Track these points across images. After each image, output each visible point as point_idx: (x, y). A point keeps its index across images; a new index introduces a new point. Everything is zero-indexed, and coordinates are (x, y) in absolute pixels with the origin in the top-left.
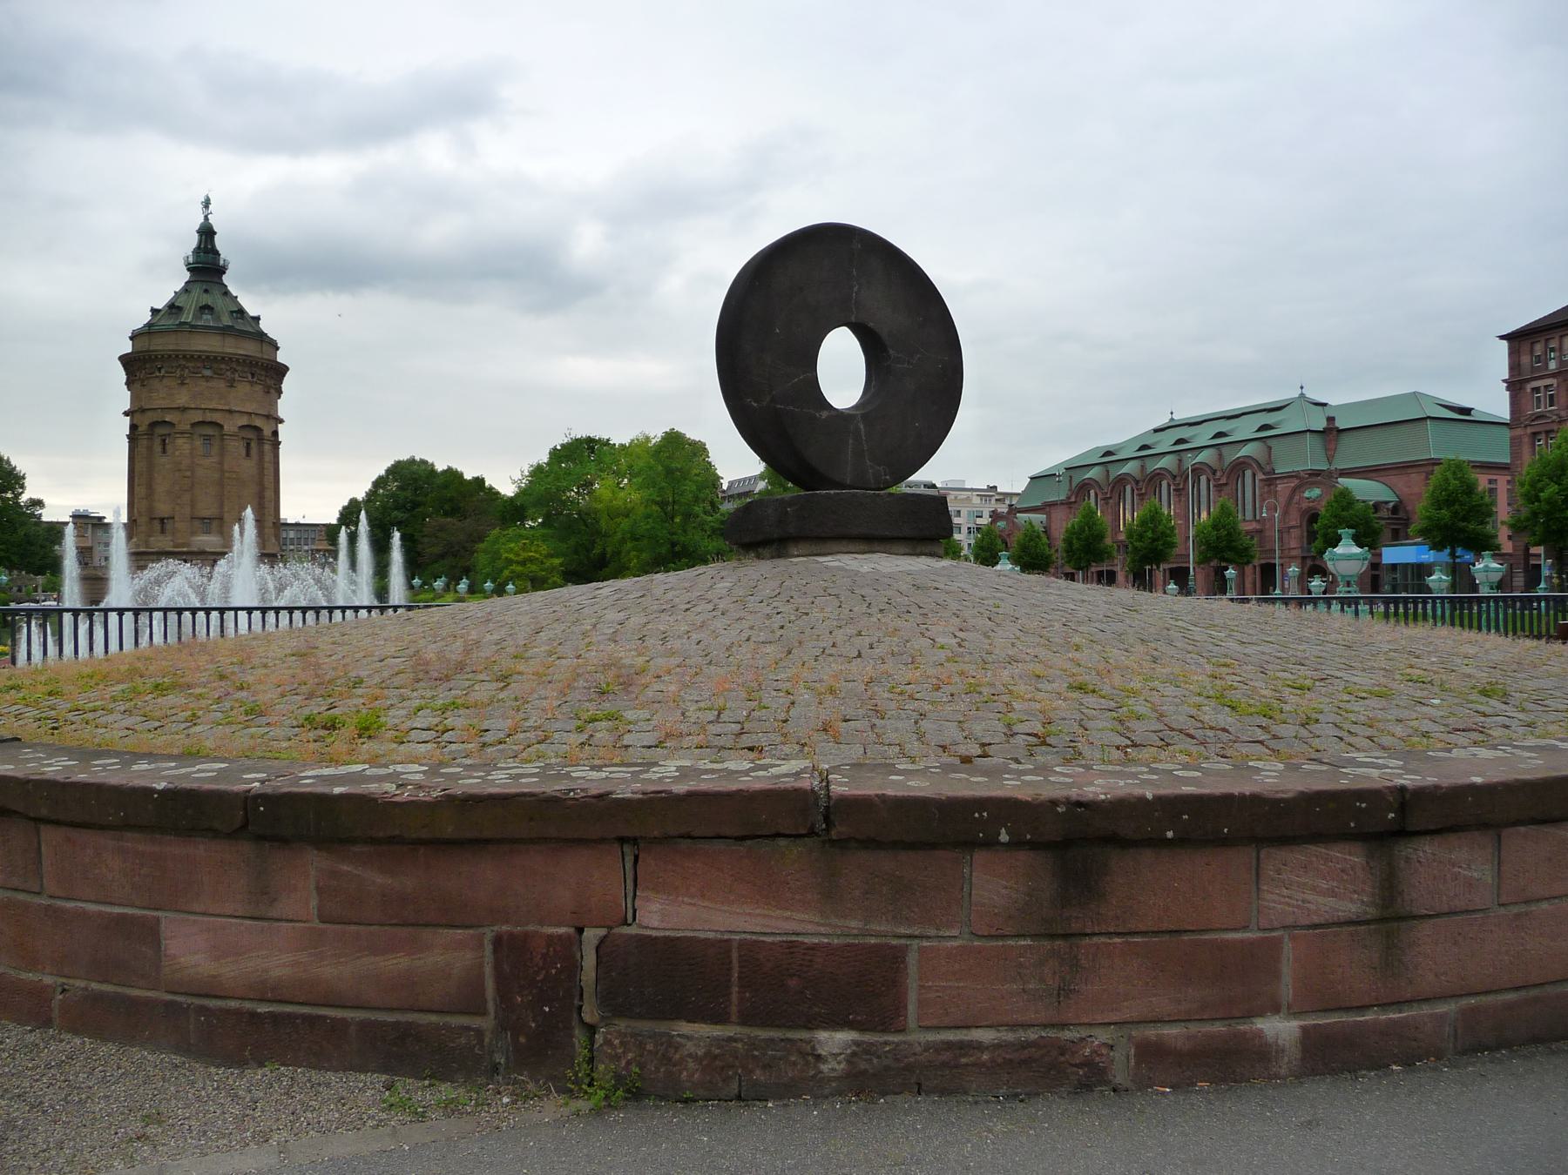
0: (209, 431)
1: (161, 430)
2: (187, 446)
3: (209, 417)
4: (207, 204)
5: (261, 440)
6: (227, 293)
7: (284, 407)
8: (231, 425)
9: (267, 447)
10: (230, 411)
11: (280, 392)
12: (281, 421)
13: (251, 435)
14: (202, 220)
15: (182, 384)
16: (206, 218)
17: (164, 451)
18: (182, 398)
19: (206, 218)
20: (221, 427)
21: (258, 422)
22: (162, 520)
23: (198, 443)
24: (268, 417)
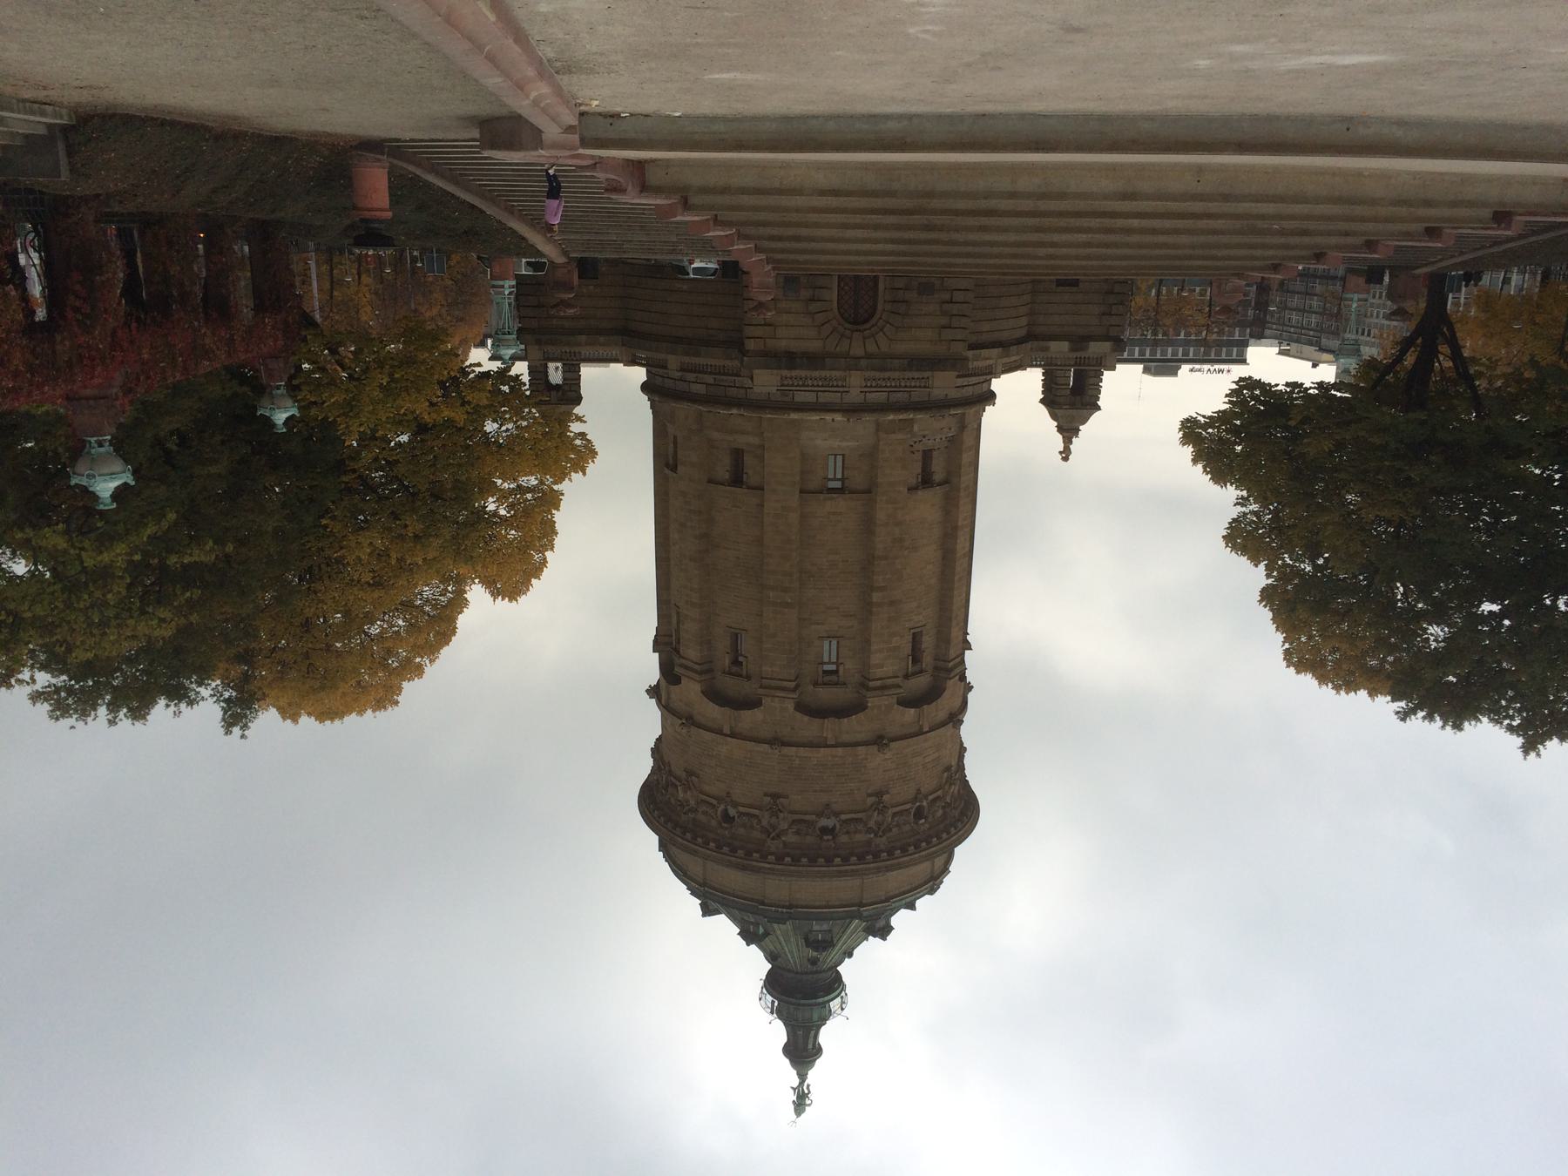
0: (826, 695)
1: (922, 682)
2: (876, 659)
3: (830, 728)
4: (801, 1101)
5: (706, 670)
6: (771, 957)
7: (649, 722)
8: (778, 712)
9: (692, 652)
10: (776, 742)
11: (656, 752)
12: (654, 692)
13: (730, 685)
14: (813, 1075)
15: (879, 794)
16: (802, 1077)
17: (916, 639)
18: (879, 763)
19: (802, 1077)
20: (801, 707)
21: (712, 712)
22: (926, 481)
23: (850, 666)
24: (689, 720)
